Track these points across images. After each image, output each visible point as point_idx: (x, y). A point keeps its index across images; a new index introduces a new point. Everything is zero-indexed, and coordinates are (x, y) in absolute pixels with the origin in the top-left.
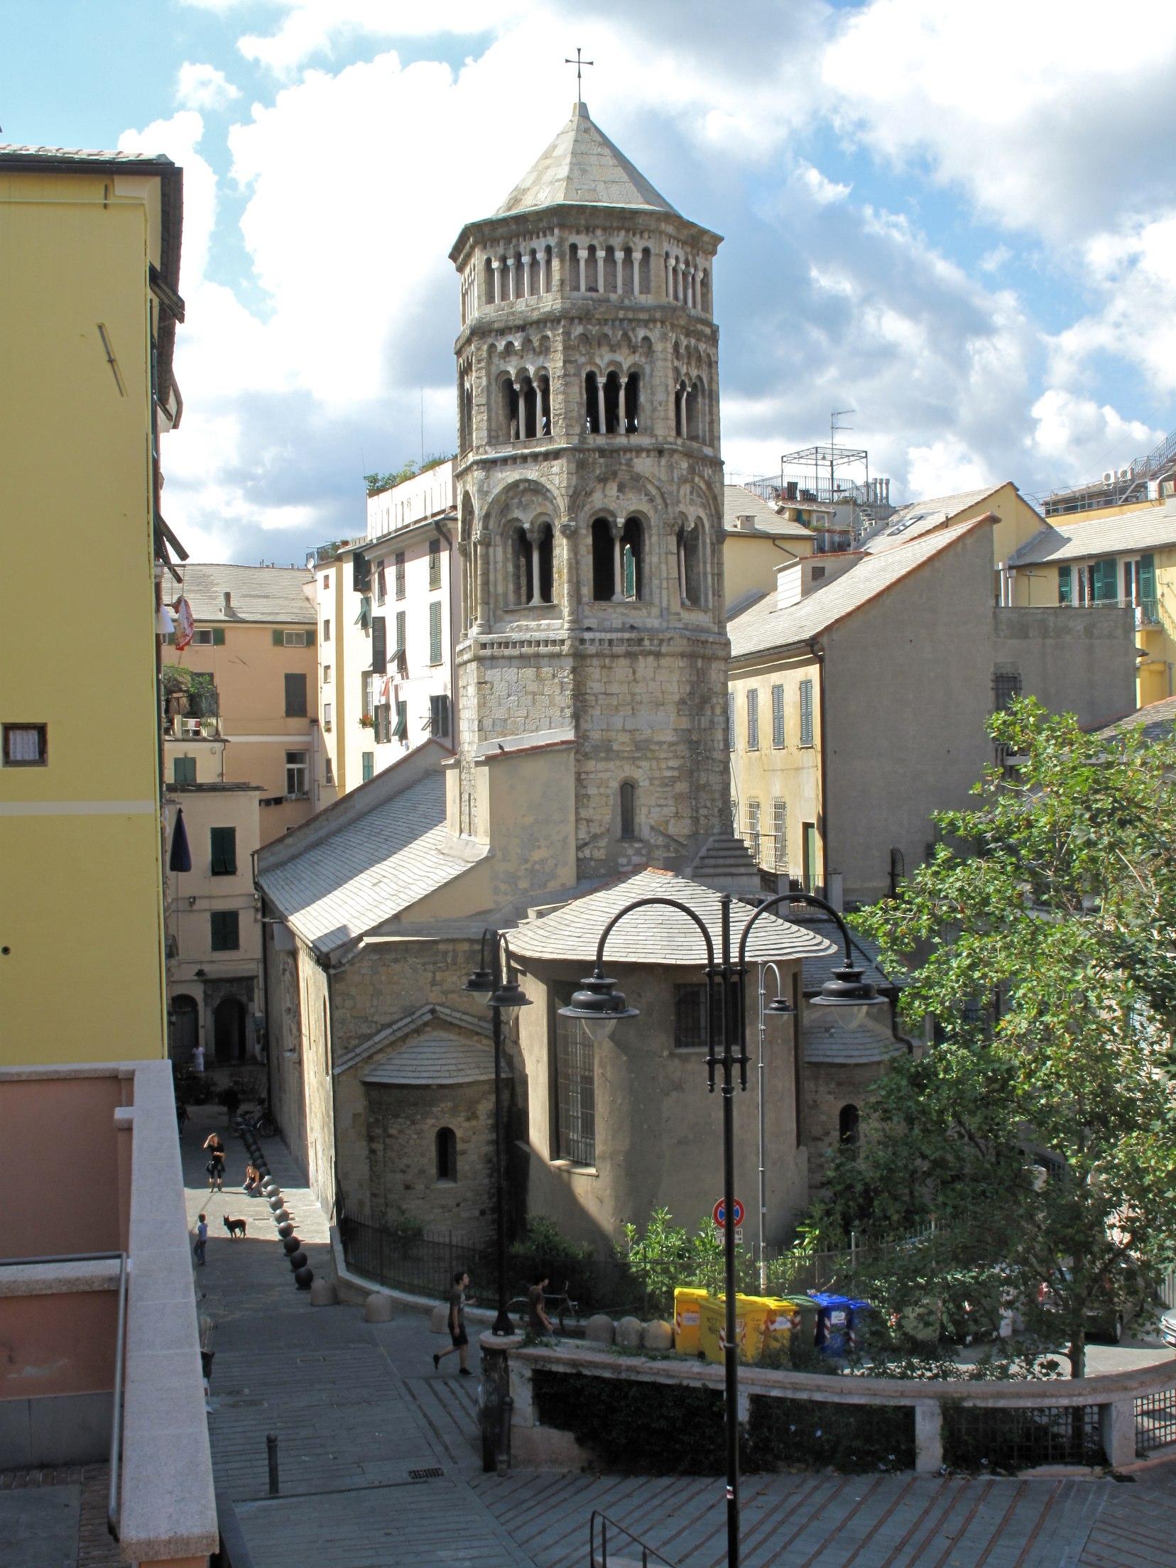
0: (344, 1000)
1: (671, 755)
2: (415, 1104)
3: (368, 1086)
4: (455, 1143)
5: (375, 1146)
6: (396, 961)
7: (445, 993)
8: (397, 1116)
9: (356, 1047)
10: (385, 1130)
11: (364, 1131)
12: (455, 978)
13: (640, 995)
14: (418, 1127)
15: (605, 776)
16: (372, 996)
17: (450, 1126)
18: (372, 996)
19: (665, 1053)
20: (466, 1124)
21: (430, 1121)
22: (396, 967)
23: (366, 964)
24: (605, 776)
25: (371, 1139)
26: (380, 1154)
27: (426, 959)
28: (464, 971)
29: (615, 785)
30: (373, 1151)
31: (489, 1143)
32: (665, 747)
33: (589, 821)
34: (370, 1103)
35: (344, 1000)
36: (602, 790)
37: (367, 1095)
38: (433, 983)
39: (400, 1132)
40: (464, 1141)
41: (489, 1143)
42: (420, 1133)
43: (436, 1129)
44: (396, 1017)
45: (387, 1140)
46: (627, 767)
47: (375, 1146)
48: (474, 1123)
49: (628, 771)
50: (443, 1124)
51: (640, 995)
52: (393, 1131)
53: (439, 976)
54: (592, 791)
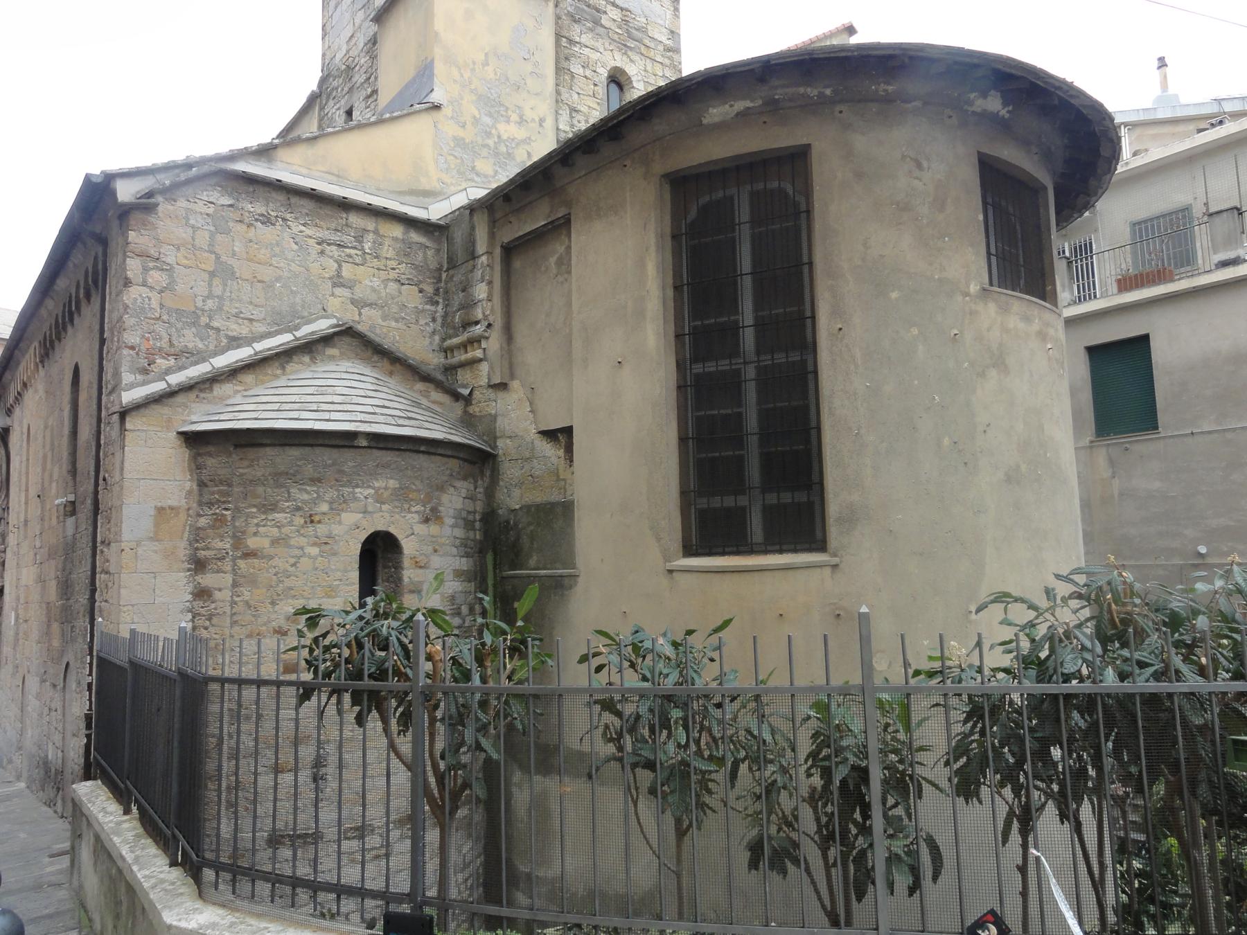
0: (146, 270)
1: (667, 62)
2: (316, 481)
3: (194, 440)
4: (398, 567)
5: (207, 580)
6: (267, 220)
7: (359, 304)
8: (272, 507)
9: (168, 371)
10: (238, 541)
11: (183, 550)
12: (376, 283)
13: (919, 166)
14: (322, 529)
15: (594, 56)
16: (212, 274)
17: (392, 530)
18: (212, 274)
19: (974, 288)
20: (421, 529)
21: (349, 518)
22: (265, 233)
23: (200, 207)
24: (594, 56)
25: (199, 565)
26: (223, 596)
27: (326, 234)
28: (393, 275)
29: (604, 73)
30: (202, 594)
31: (458, 574)
32: (661, 48)
33: (573, 110)
34: (202, 485)
35: (146, 270)
36: (588, 73)
37: (197, 467)
38: (338, 281)
39: (275, 542)
40: (418, 566)
41: (458, 574)
42: (324, 543)
43: (363, 536)
44: (262, 328)
45: (242, 563)
46: (618, 55)
47: (207, 580)
48: (434, 529)
49: (619, 61)
50: (380, 523)
51: (919, 166)
52: (252, 543)
53: (347, 271)
54: (576, 69)
